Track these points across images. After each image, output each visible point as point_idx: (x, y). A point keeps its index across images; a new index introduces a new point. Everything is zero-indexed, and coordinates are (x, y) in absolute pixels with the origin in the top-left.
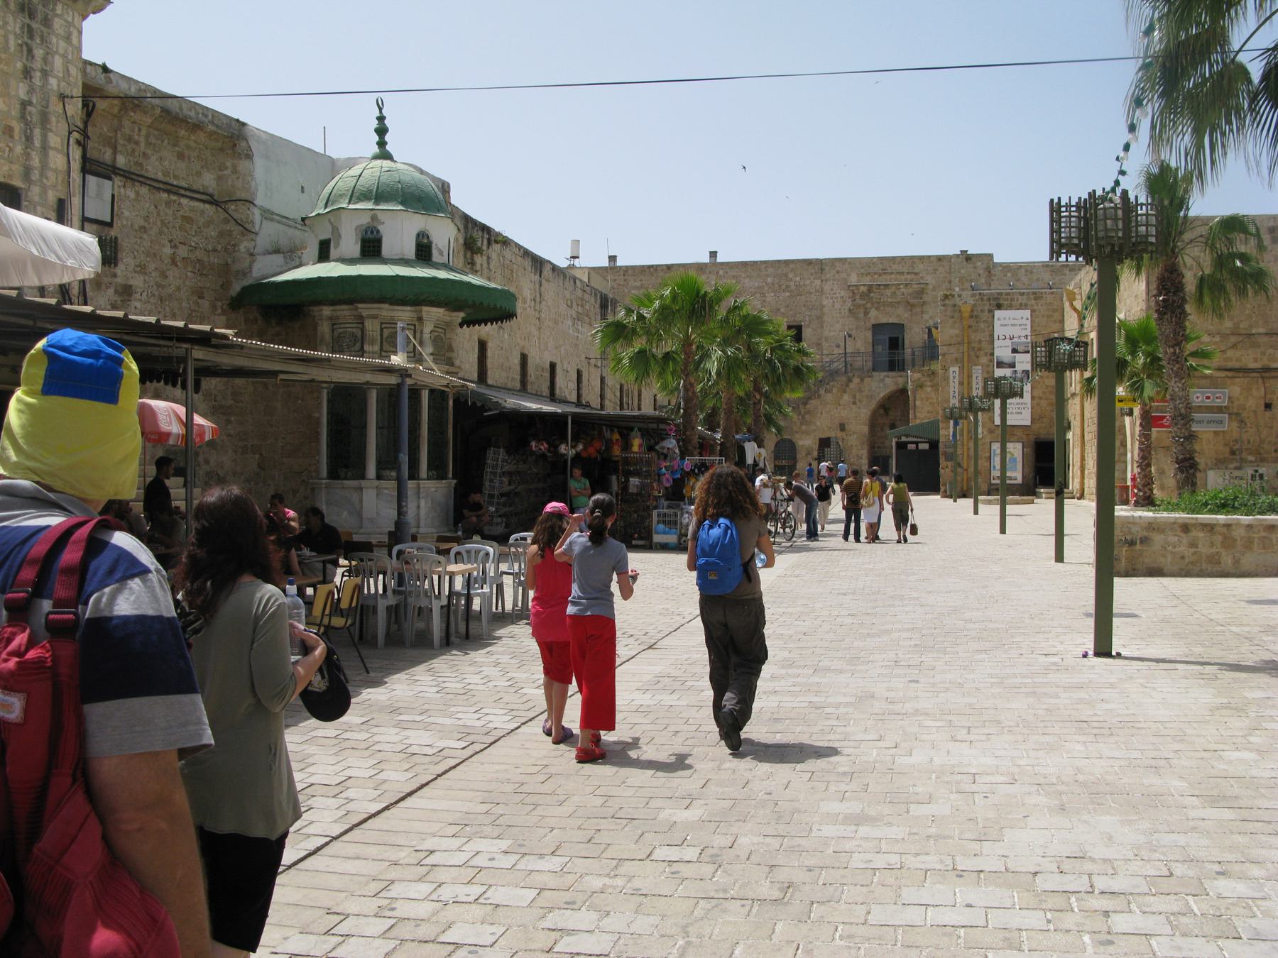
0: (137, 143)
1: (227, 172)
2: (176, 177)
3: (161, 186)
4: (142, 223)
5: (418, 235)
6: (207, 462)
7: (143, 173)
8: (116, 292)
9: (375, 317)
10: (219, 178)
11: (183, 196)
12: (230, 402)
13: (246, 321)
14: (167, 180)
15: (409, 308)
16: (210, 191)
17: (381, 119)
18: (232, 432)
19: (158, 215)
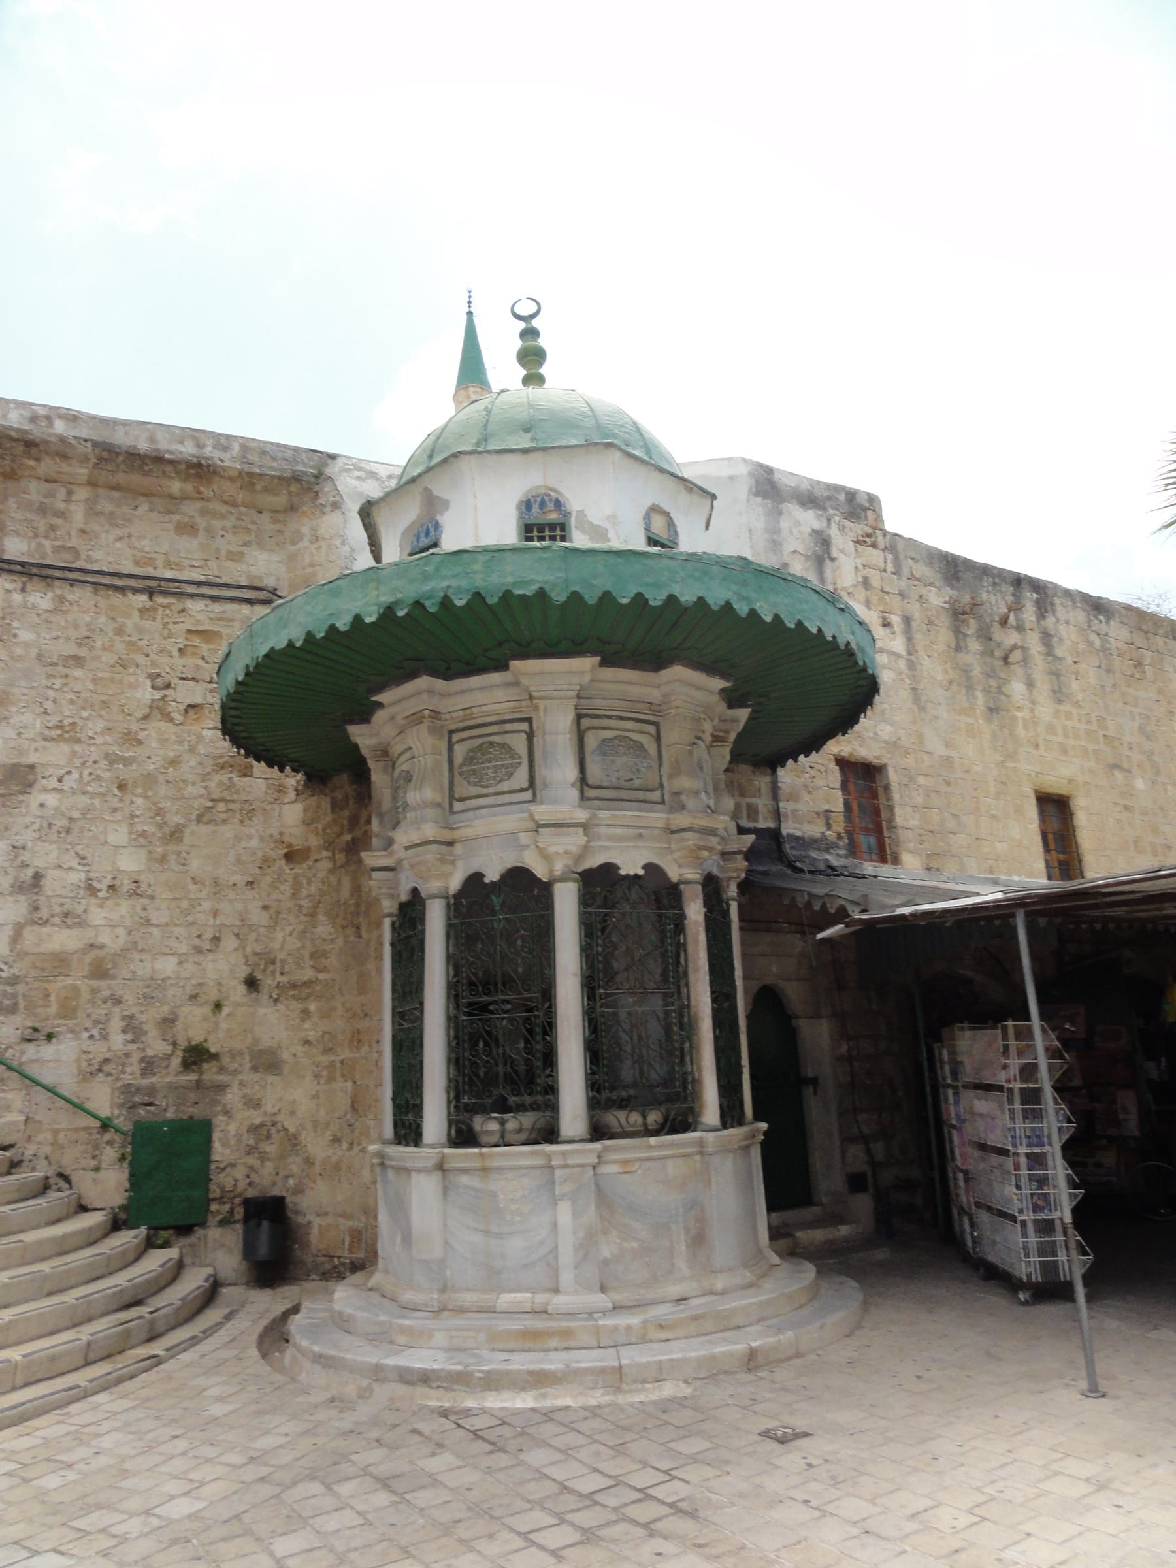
0: (61, 515)
1: (305, 543)
3: (132, 583)
4: (71, 649)
5: (527, 505)
6: (253, 1103)
9: (416, 719)
10: (292, 558)
11: (192, 596)
12: (308, 974)
13: (335, 805)
14: (150, 571)
15: (495, 677)
17: (530, 333)
18: (312, 1035)
19: (120, 631)
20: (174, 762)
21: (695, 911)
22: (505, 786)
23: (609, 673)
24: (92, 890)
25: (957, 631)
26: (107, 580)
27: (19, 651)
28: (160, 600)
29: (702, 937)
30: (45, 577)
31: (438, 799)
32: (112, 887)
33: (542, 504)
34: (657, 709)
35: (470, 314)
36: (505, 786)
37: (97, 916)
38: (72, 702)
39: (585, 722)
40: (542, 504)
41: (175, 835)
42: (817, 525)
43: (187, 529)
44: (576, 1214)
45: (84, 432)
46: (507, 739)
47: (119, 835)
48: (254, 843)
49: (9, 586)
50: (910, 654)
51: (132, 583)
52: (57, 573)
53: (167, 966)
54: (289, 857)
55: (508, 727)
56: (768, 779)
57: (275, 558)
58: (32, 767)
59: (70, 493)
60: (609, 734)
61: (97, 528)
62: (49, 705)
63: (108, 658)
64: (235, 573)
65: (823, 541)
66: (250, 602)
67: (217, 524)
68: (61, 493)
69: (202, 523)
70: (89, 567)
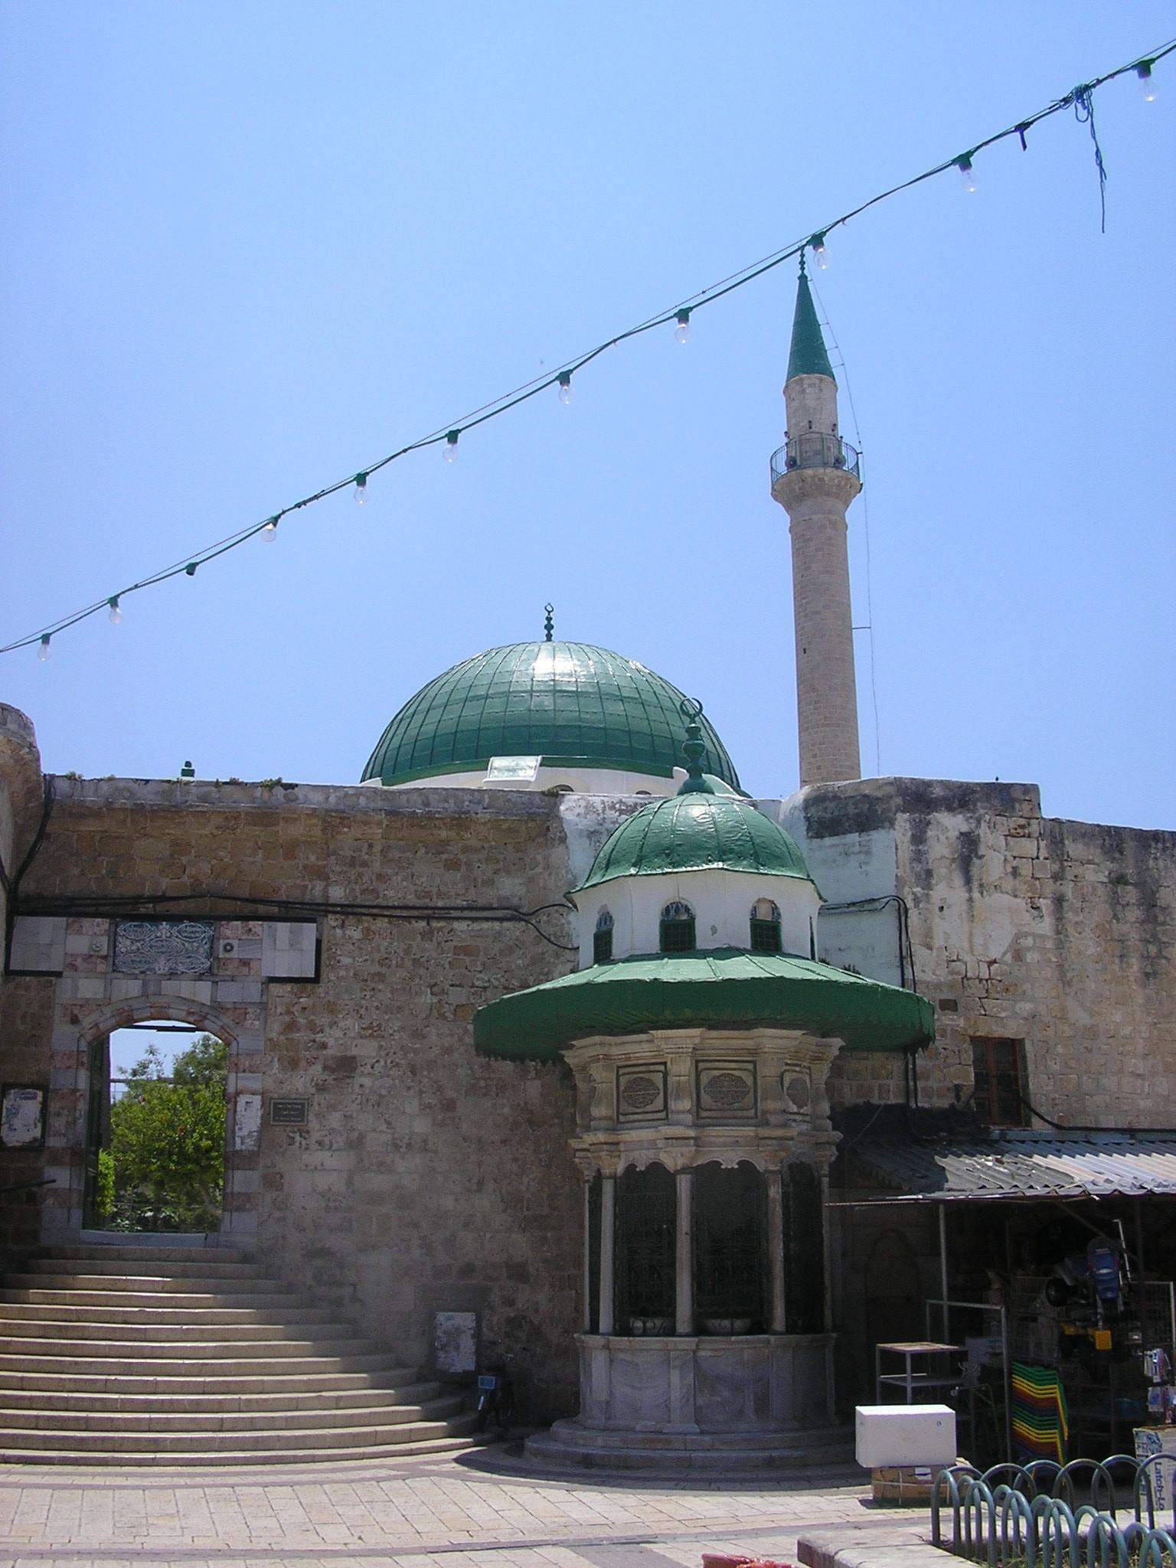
0: (364, 864)
2: (440, 895)
3: (415, 913)
4: (376, 968)
5: (667, 910)
6: (510, 1302)
7: (380, 901)
8: (325, 1068)
9: (595, 1059)
10: (531, 880)
15: (643, 1037)
16: (515, 901)
20: (449, 1051)
21: (775, 1192)
22: (649, 1108)
23: (714, 1033)
24: (397, 1147)
25: (1115, 901)
26: (398, 913)
27: (342, 973)
28: (435, 924)
29: (779, 1209)
30: (356, 914)
31: (610, 1113)
32: (409, 1146)
33: (677, 911)
34: (755, 1051)
35: (803, 279)
36: (649, 1108)
37: (401, 1166)
38: (377, 1008)
39: (701, 1065)
40: (677, 911)
41: (449, 1106)
42: (965, 828)
43: (452, 865)
44: (682, 1378)
45: (380, 804)
46: (652, 1076)
47: (413, 1107)
48: (506, 1110)
49: (334, 924)
50: (1058, 932)
51: (415, 913)
52: (364, 910)
53: (448, 1203)
54: (530, 1122)
55: (652, 1068)
56: (900, 1063)
57: (517, 881)
58: (354, 1058)
59: (371, 846)
60: (717, 1073)
61: (390, 871)
62: (362, 1011)
63: (401, 973)
64: (489, 896)
65: (969, 844)
66: (501, 920)
67: (475, 857)
68: (365, 849)
69: (463, 858)
70: (385, 903)
